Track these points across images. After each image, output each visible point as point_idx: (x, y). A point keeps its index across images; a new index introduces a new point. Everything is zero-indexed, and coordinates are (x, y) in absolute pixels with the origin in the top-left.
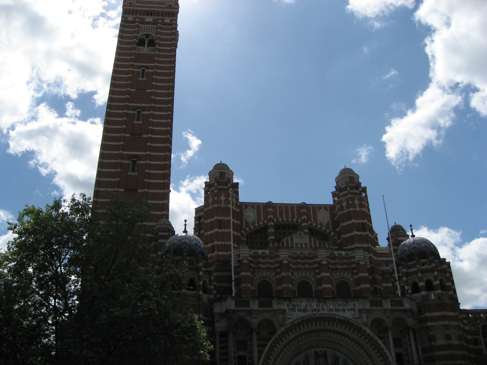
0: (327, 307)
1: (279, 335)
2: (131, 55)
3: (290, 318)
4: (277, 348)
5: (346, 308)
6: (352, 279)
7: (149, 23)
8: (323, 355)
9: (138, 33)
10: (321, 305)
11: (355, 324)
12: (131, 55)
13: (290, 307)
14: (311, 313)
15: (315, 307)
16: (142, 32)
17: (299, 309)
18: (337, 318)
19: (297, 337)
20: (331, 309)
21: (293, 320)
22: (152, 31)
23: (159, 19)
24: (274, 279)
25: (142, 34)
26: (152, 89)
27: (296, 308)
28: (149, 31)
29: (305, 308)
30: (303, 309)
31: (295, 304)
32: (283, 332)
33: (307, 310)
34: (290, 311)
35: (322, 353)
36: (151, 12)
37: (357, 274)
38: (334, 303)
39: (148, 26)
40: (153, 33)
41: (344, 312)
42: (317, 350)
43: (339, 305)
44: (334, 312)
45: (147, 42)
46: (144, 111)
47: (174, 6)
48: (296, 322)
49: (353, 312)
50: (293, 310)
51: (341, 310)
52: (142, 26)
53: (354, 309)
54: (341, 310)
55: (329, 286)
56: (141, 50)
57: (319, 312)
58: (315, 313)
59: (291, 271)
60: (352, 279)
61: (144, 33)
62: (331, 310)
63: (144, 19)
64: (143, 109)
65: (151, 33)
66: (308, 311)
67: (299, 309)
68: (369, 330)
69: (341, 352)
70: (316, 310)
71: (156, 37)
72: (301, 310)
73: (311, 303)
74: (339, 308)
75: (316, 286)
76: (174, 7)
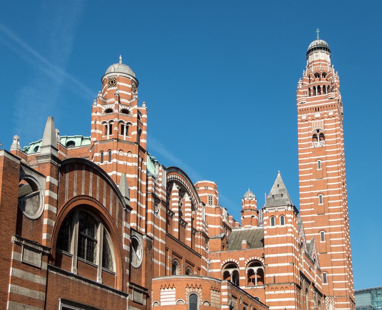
2: (309, 150)
7: (318, 118)
9: (311, 131)
12: (309, 150)
16: (314, 128)
22: (321, 126)
23: (324, 114)
25: (314, 130)
26: (327, 177)
28: (319, 127)
36: (318, 108)
39: (317, 121)
40: (322, 127)
45: (318, 136)
46: (324, 195)
47: (334, 98)
52: (313, 123)
56: (315, 144)
61: (315, 129)
63: (314, 115)
64: (323, 193)
65: (320, 128)
71: (325, 131)
76: (334, 99)
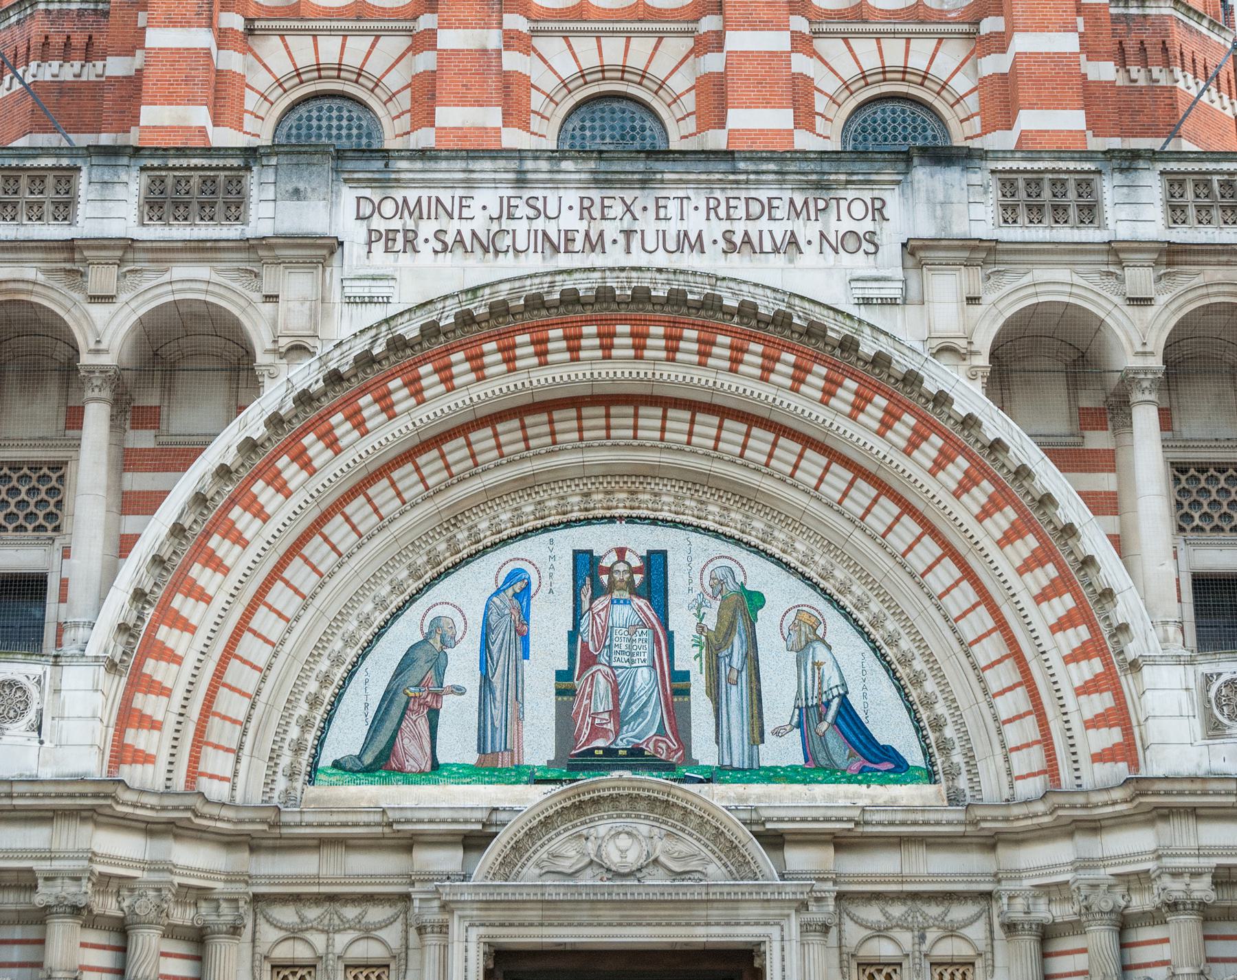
0: (662, 225)
1: (275, 421)
3: (371, 301)
4: (261, 514)
5: (807, 231)
6: (961, 84)
8: (638, 578)
10: (617, 209)
11: (868, 348)
13: (377, 223)
14: (534, 263)
15: (570, 220)
17: (449, 239)
18: (731, 302)
19: (436, 441)
20: (693, 239)
21: (392, 310)
24: (395, 80)
27: (427, 229)
29: (495, 227)
30: (474, 234)
31: (419, 201)
32: (305, 399)
33: (508, 240)
34: (378, 247)
35: (636, 563)
37: (999, 43)
38: (718, 194)
41: (791, 261)
42: (599, 540)
43: (755, 208)
44: (712, 261)
48: (410, 329)
49: (860, 264)
50: (399, 245)
51: (768, 246)
53: (871, 237)
54: (768, 246)
55: (780, 118)
57: (596, 260)
58: (563, 261)
59: (516, 22)
60: (961, 84)
62: (692, 243)
66: (517, 252)
67: (449, 239)
68: (977, 388)
69: (779, 562)
70: (578, 245)
72: (460, 241)
73: (539, 193)
74: (753, 228)
75: (693, 129)
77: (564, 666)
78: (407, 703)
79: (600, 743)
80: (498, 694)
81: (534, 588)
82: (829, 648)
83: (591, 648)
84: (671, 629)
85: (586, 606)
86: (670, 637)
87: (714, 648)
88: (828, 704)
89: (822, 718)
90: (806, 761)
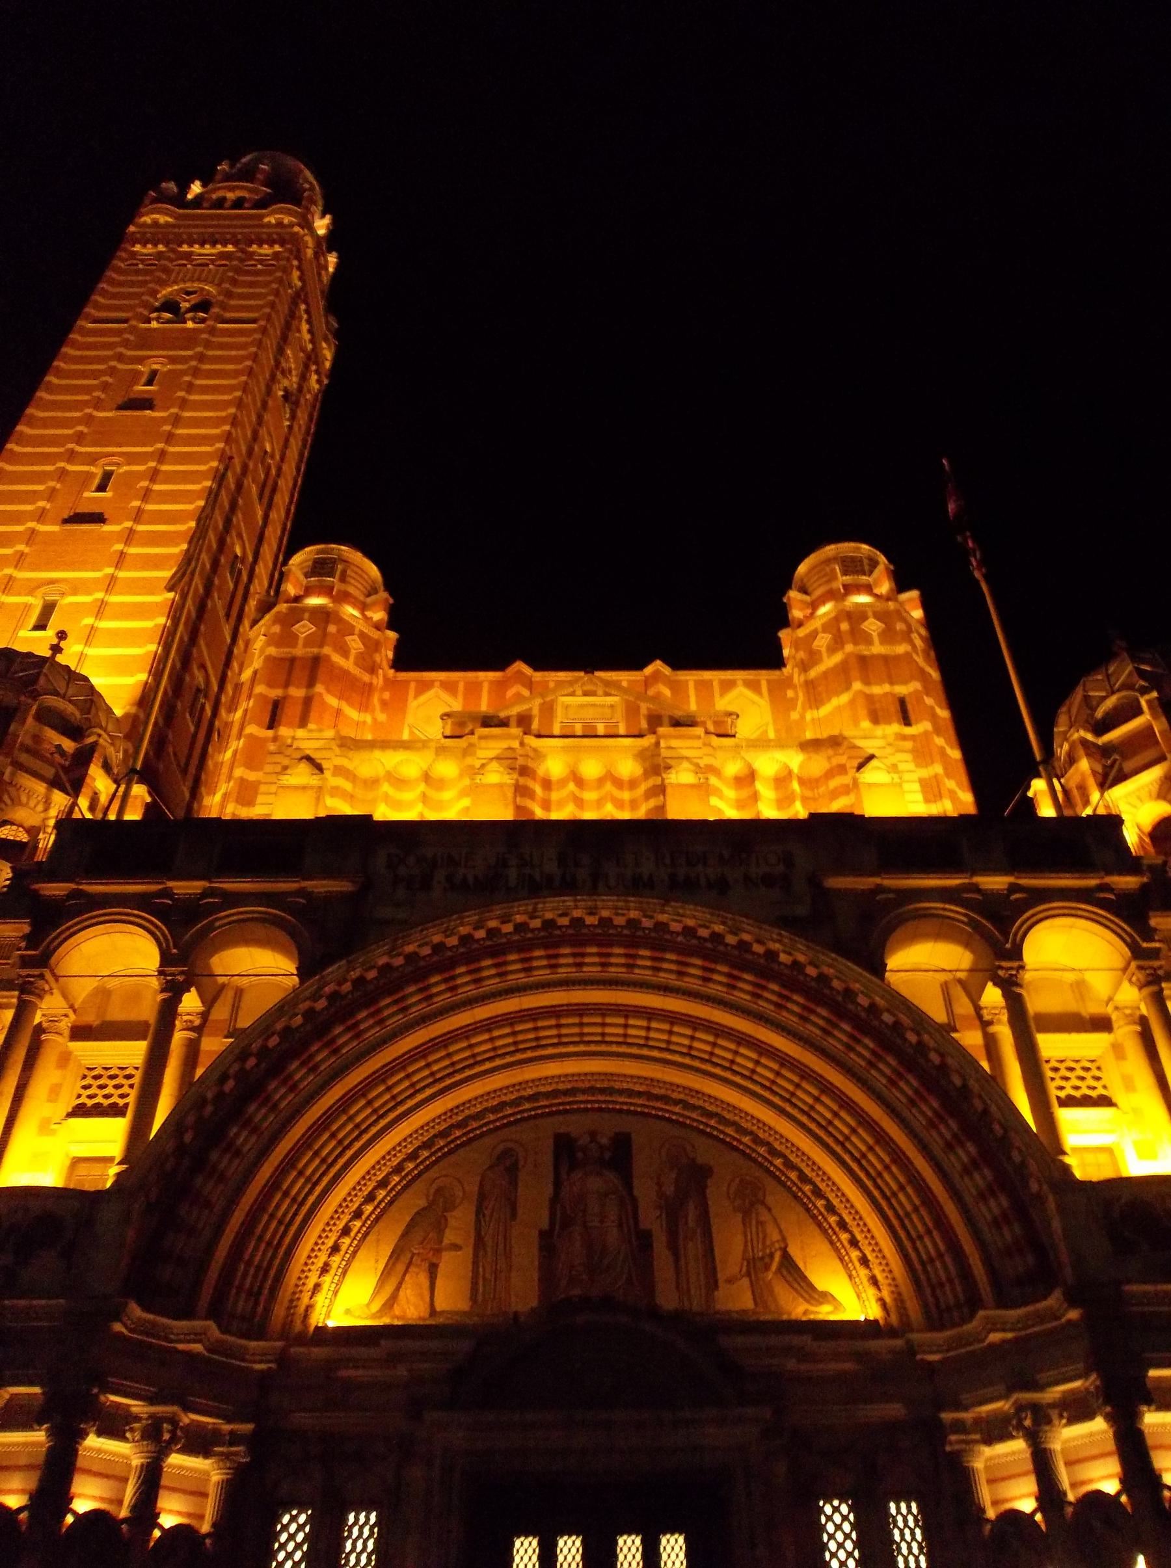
15: (551, 867)
27: (440, 875)
35: (604, 1141)
77: (545, 1225)
78: (412, 1258)
79: (577, 1292)
80: (489, 1250)
81: (521, 1163)
82: (770, 1210)
83: (569, 1212)
84: (636, 1193)
85: (564, 1176)
86: (634, 1200)
87: (673, 1210)
88: (772, 1256)
89: (767, 1267)
90: (756, 1304)
